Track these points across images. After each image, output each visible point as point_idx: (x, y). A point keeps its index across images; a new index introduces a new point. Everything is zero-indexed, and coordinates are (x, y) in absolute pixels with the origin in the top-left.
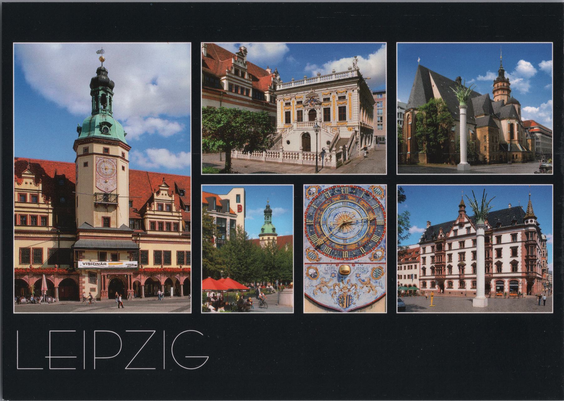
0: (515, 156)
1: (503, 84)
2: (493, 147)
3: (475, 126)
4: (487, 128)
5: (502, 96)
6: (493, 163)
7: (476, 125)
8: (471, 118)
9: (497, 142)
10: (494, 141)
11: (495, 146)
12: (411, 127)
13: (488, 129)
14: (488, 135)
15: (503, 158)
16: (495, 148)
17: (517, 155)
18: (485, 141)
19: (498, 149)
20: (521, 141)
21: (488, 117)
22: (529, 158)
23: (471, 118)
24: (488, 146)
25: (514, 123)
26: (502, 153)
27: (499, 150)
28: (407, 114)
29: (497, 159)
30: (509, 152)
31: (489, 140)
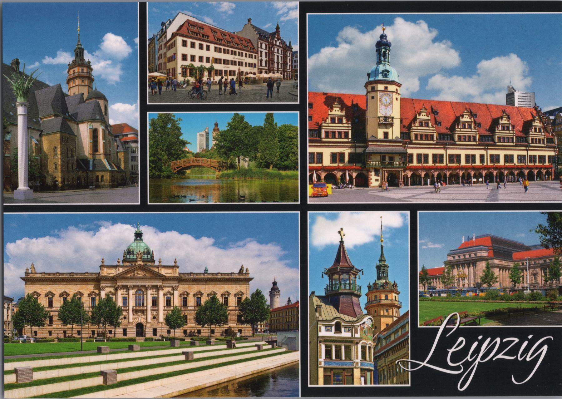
1: (83, 70)
2: (68, 164)
3: (39, 133)
4: (58, 135)
5: (80, 87)
7: (42, 131)
8: (35, 120)
9: (73, 157)
10: (70, 155)
11: (70, 162)
14: (59, 147)
15: (83, 180)
16: (70, 165)
17: (102, 177)
18: (56, 154)
19: (75, 167)
20: (110, 155)
21: (59, 119)
22: (121, 180)
23: (35, 120)
24: (59, 163)
25: (98, 128)
26: (80, 173)
29: (73, 182)
30: (90, 171)
31: (61, 154)
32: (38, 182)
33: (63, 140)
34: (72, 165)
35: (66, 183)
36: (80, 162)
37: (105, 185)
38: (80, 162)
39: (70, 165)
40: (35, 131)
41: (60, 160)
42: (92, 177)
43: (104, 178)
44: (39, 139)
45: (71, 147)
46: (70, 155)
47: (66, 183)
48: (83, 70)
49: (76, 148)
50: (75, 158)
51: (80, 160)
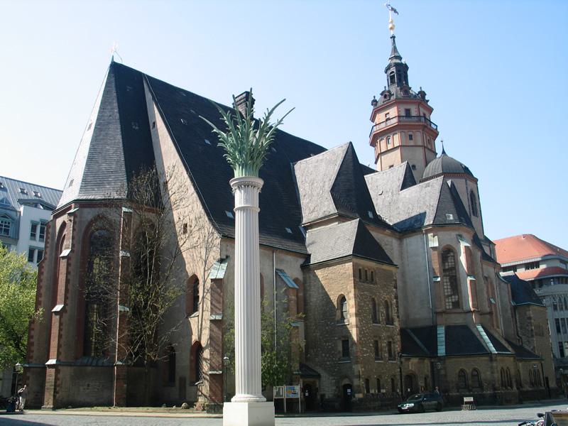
3: (301, 261)
4: (349, 265)
6: (377, 404)
8: (289, 231)
9: (389, 321)
10: (382, 317)
11: (384, 334)
12: (68, 265)
13: (351, 272)
14: (352, 295)
15: (421, 383)
19: (397, 347)
20: (491, 313)
21: (351, 227)
22: (532, 384)
23: (289, 231)
25: (453, 244)
26: (413, 364)
28: (59, 222)
29: (394, 389)
30: (440, 359)
31: (357, 315)
32: (298, 388)
33: (360, 278)
34: (389, 343)
36: (413, 335)
38: (413, 335)
40: (289, 258)
42: (446, 375)
44: (300, 277)
45: (385, 296)
46: (382, 317)
49: (396, 298)
50: (396, 323)
51: (415, 330)
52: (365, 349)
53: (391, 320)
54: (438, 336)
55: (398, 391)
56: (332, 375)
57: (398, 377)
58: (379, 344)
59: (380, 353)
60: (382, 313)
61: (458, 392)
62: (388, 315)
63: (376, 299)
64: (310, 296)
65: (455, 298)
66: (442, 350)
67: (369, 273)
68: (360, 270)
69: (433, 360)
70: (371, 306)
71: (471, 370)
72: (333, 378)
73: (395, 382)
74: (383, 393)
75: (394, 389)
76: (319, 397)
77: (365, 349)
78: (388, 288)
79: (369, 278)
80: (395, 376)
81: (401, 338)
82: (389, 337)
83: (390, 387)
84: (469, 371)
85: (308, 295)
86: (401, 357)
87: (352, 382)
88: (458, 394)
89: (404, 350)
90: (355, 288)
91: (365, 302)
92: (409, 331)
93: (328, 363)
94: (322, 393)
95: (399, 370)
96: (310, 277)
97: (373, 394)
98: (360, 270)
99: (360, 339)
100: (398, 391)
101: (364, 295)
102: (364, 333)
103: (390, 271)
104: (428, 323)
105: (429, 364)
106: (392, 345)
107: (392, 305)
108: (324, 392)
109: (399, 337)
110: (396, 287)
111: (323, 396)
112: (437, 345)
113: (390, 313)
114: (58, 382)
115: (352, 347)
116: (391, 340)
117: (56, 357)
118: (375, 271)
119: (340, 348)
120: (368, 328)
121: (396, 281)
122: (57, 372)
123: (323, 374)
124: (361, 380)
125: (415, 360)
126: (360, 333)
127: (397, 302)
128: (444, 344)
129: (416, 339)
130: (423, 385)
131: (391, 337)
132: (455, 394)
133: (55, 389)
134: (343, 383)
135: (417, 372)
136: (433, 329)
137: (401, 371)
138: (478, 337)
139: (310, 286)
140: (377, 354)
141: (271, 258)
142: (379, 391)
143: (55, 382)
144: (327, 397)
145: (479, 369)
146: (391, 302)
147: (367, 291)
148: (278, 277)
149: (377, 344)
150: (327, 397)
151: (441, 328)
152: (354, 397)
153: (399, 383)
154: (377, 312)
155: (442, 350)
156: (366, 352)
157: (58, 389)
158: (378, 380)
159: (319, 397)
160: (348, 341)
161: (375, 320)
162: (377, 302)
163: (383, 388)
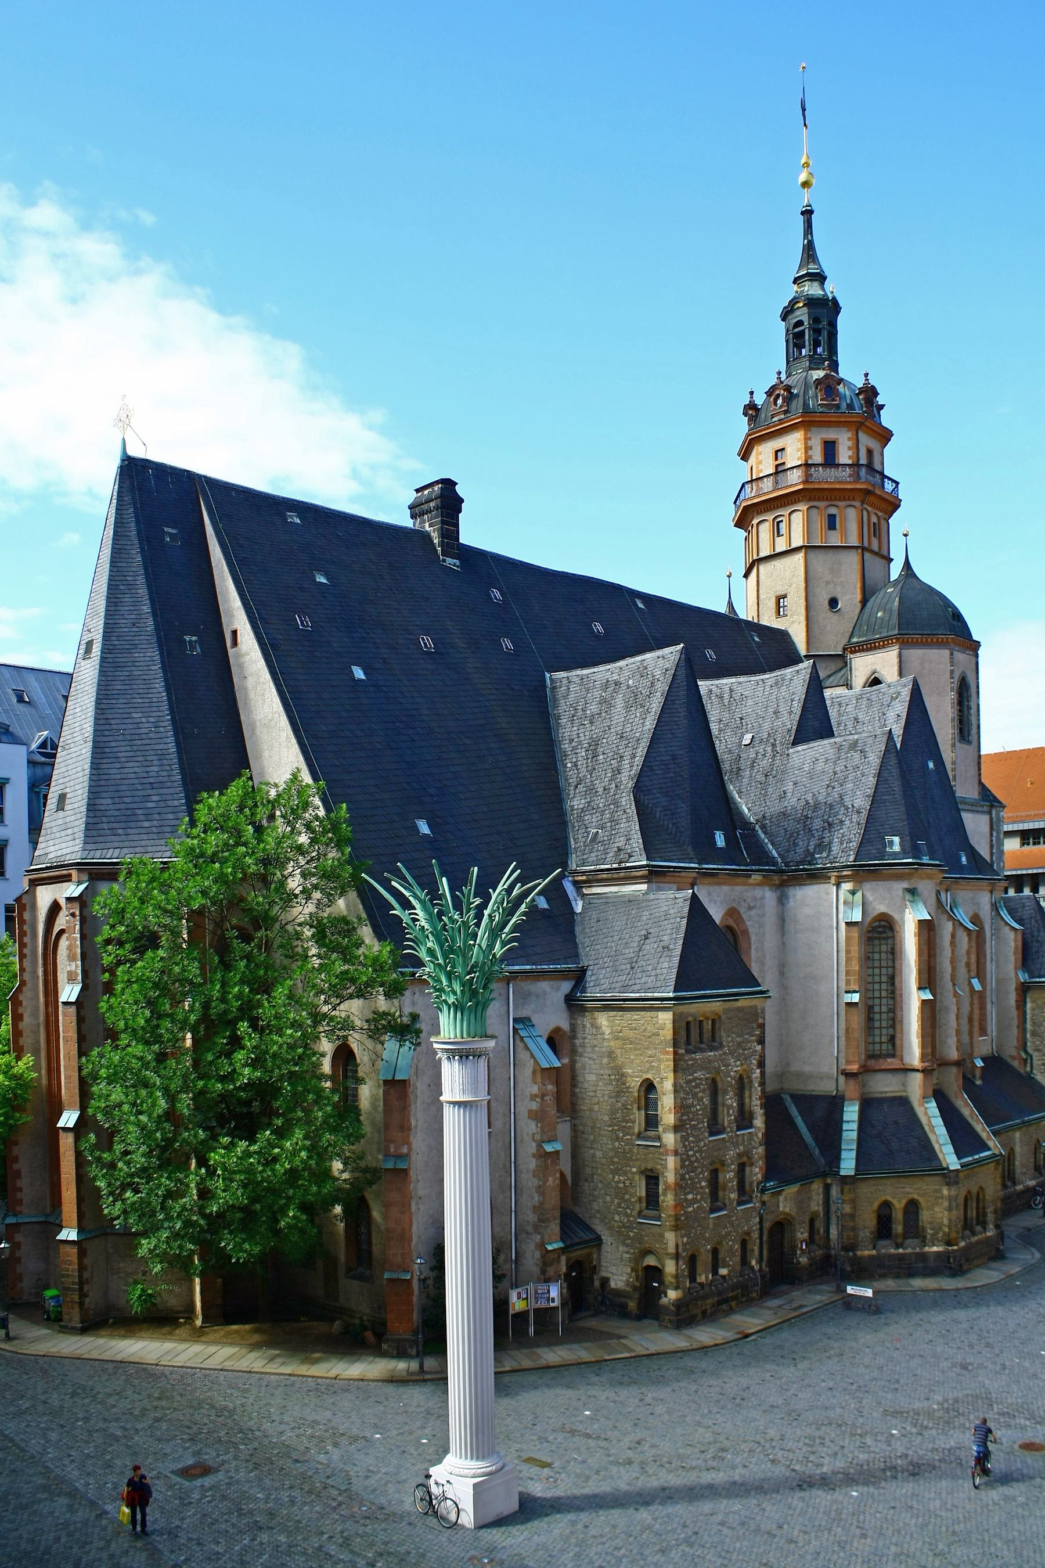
0: (898, 1215)
1: (830, 448)
3: (566, 987)
5: (820, 561)
7: (579, 977)
10: (728, 1117)
13: (668, 1033)
14: (668, 1085)
16: (729, 1175)
17: (913, 1207)
18: (652, 1122)
19: (756, 1173)
24: (670, 1176)
27: (767, 1178)
33: (688, 1042)
35: (702, 1279)
36: (794, 1111)
37: (923, 1257)
38: (794, 1111)
39: (729, 1175)
41: (671, 1162)
43: (925, 1216)
46: (728, 1117)
47: (702, 1279)
48: (830, 448)
49: (761, 1064)
52: (690, 1196)
53: (747, 1115)
54: (844, 1134)
55: (753, 1263)
56: (624, 1244)
57: (755, 1235)
58: (721, 1176)
59: (721, 1194)
60: (730, 1107)
61: (874, 1248)
62: (741, 1105)
63: (718, 1079)
64: (584, 1067)
65: (891, 1032)
66: (848, 1165)
67: (708, 1026)
68: (688, 1023)
69: (829, 1181)
70: (706, 1101)
71: (904, 1202)
72: (625, 1249)
73: (749, 1247)
74: (723, 1277)
75: (744, 1261)
76: (597, 1283)
77: (690, 1196)
78: (744, 1050)
79: (707, 1036)
80: (748, 1233)
81: (767, 1150)
82: (740, 1155)
83: (738, 1259)
84: (899, 1205)
85: (578, 1065)
86: (763, 1191)
87: (663, 1266)
88: (874, 1252)
89: (770, 1173)
90: (675, 1071)
91: (695, 1096)
92: (788, 1099)
93: (617, 1218)
94: (604, 1274)
95: (757, 1220)
96: (584, 1026)
97: (701, 1284)
98: (688, 1023)
99: (683, 1177)
100: (753, 1263)
101: (695, 1079)
102: (692, 1163)
103: (751, 1007)
104: (828, 1087)
105: (821, 1190)
106: (747, 1169)
107: (751, 1082)
108: (609, 1275)
109: (761, 1150)
110: (761, 1041)
111: (605, 1281)
112: (839, 1150)
113: (747, 1100)
114: (86, 1275)
115: (665, 1194)
116: (745, 1159)
117: (75, 1222)
118: (720, 1017)
119: (642, 1192)
120: (700, 1151)
121: (762, 1026)
122: (82, 1254)
123: (606, 1238)
124: (681, 1262)
125: (792, 1190)
126: (683, 1166)
127: (763, 1074)
128: (854, 1147)
129: (799, 1121)
130: (806, 1235)
131: (747, 1154)
132: (867, 1253)
133: (81, 1289)
134: (645, 1264)
135: (793, 1214)
136: (835, 1104)
137: (761, 1223)
138: (927, 1128)
139: (583, 1046)
140: (714, 1195)
141: (505, 997)
142: (715, 1272)
143: (80, 1276)
144: (613, 1285)
145: (921, 1200)
146: (749, 1077)
147: (702, 1069)
148: (517, 1037)
149: (717, 1177)
150: (613, 1285)
151: (850, 1109)
152: (666, 1296)
153: (756, 1249)
154: (720, 1108)
155: (848, 1165)
156: (694, 1200)
157: (86, 1288)
158: (715, 1252)
159: (597, 1283)
160: (657, 1178)
161: (715, 1128)
162: (720, 1086)
163: (724, 1267)
